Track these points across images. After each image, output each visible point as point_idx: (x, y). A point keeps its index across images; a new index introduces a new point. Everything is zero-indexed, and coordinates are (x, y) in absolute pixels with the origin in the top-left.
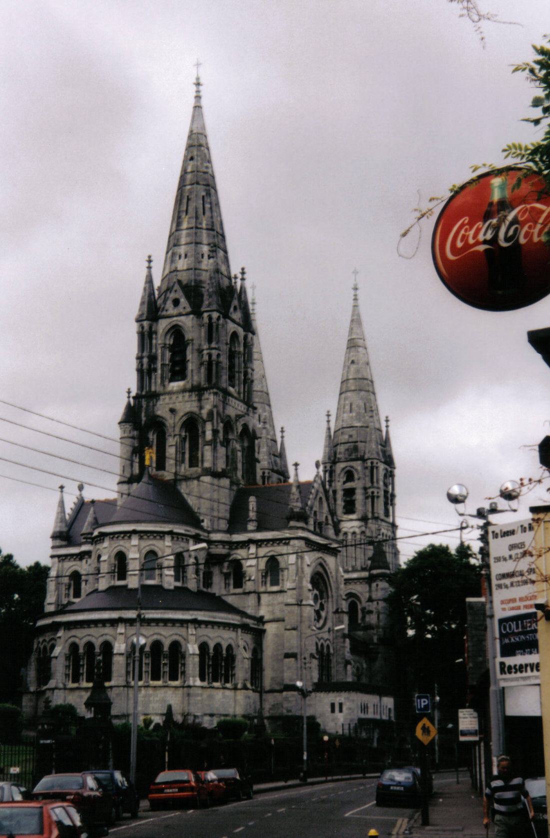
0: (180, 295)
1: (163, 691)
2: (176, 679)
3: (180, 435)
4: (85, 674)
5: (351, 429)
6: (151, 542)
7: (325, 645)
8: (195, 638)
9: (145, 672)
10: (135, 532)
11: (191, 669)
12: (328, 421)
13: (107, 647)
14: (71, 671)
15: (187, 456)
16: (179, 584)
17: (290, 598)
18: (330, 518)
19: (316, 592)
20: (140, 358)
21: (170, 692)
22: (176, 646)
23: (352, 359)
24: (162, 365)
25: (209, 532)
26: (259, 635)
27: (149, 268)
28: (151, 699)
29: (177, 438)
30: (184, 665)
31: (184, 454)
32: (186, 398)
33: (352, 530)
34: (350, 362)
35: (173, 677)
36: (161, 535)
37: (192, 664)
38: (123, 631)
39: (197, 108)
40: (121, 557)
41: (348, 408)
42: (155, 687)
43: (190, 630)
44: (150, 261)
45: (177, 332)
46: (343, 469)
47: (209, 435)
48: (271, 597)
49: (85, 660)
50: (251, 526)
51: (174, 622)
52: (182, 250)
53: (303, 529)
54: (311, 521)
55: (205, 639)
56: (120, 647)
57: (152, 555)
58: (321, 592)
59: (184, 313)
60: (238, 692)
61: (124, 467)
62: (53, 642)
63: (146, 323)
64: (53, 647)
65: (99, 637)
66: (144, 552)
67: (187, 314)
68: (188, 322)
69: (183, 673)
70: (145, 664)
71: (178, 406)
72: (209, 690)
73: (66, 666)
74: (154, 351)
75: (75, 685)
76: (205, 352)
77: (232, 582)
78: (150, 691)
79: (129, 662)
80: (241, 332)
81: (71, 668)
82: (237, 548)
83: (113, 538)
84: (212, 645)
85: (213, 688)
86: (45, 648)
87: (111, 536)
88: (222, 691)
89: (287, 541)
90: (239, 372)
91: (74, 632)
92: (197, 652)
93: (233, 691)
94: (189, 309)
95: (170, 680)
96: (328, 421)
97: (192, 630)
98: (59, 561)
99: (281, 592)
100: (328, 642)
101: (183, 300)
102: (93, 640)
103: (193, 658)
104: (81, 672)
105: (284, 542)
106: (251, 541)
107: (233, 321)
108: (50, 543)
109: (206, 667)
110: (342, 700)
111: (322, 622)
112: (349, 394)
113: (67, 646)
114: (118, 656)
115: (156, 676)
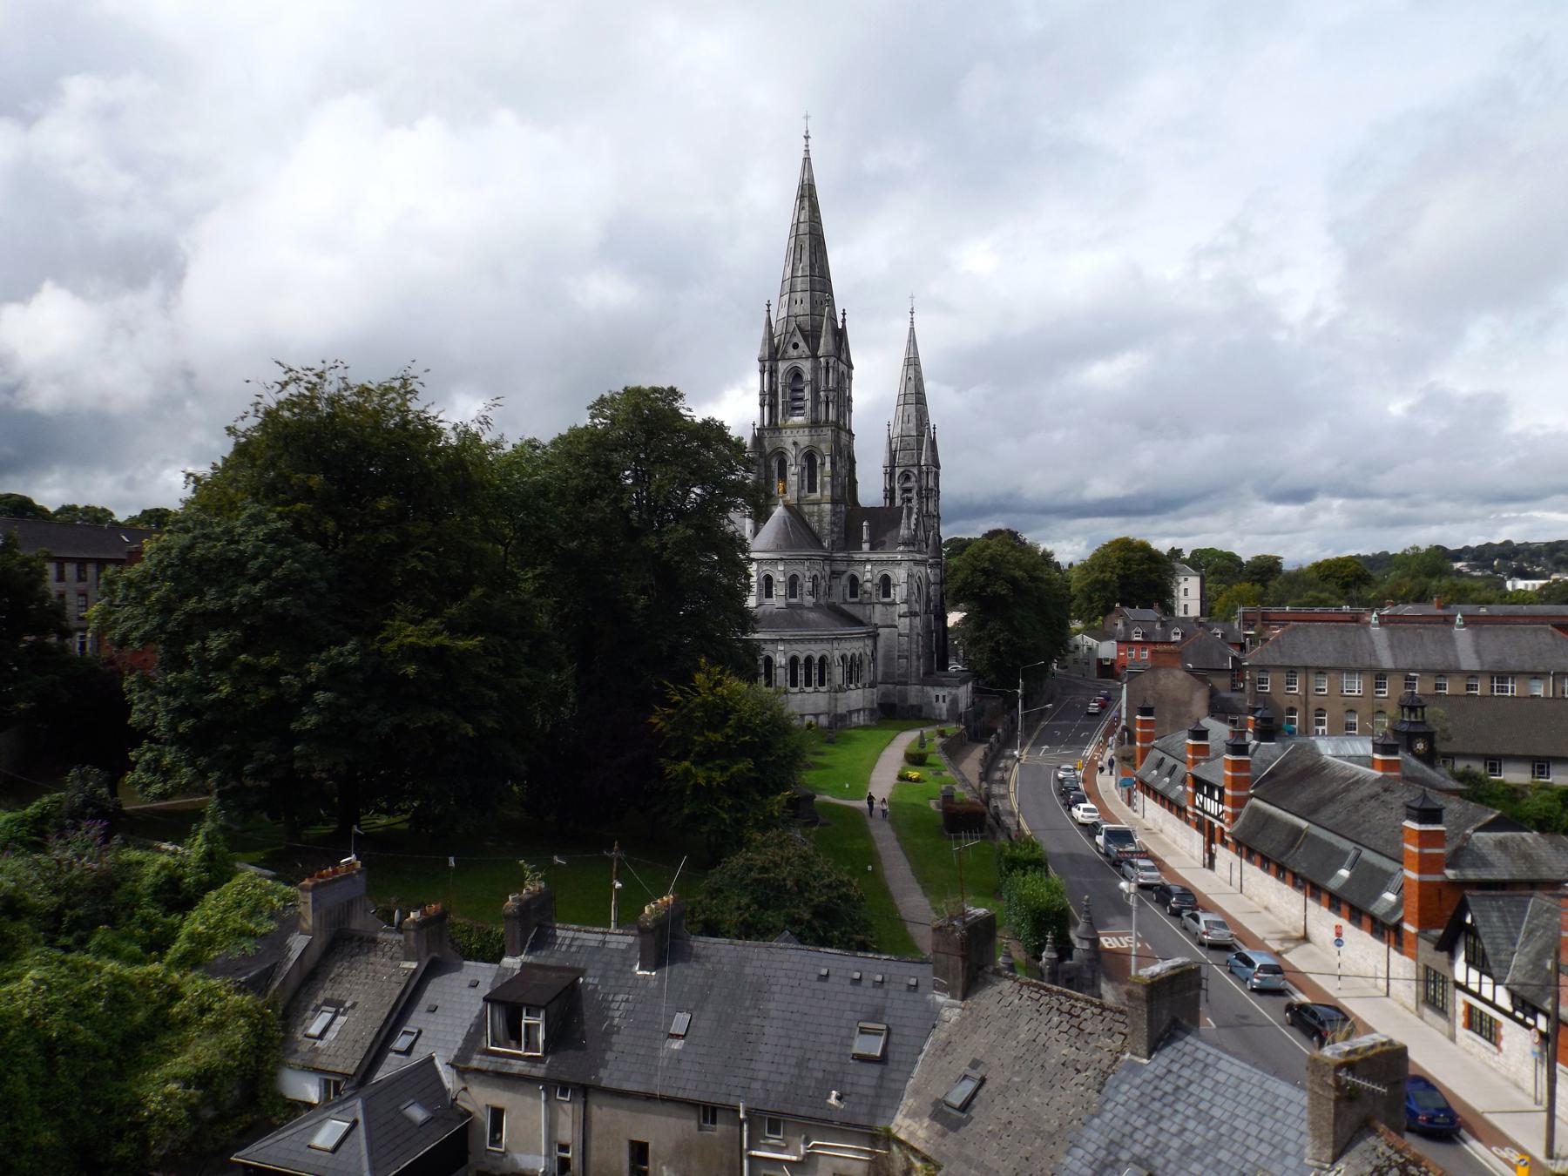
0: (798, 339)
10: (781, 559)
15: (806, 482)
20: (762, 394)
22: (823, 659)
27: (769, 311)
31: (803, 481)
32: (807, 433)
35: (822, 683)
36: (801, 561)
37: (838, 674)
38: (782, 648)
39: (807, 160)
40: (769, 579)
41: (906, 419)
44: (769, 306)
46: (902, 473)
47: (828, 466)
50: (866, 547)
52: (798, 296)
60: (866, 690)
66: (789, 575)
67: (807, 358)
68: (806, 366)
71: (798, 439)
74: (774, 387)
76: (822, 393)
77: (848, 592)
82: (854, 565)
97: (835, 645)
101: (802, 344)
106: (868, 561)
110: (946, 694)
112: (906, 407)
115: (808, 684)
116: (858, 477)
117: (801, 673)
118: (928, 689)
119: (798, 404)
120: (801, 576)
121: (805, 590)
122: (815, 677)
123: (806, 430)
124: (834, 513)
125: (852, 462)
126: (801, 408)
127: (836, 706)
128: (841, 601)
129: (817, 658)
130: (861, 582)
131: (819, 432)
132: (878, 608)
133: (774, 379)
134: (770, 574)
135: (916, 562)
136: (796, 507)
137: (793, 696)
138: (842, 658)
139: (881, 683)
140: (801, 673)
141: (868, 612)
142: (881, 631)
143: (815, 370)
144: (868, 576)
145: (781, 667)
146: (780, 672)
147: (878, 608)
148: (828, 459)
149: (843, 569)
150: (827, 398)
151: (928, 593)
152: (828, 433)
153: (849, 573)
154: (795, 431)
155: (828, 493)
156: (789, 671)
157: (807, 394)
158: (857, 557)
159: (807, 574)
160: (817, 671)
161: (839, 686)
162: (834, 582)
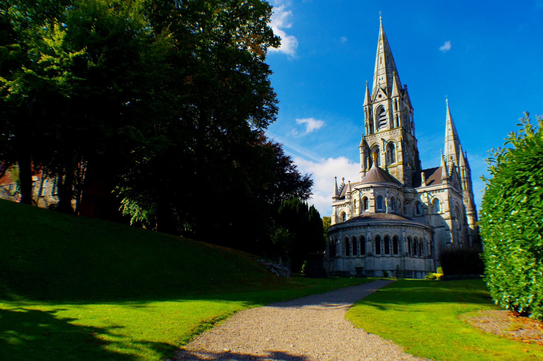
1: (391, 258)
3: (387, 150)
4: (352, 252)
10: (372, 187)
14: (345, 250)
16: (393, 211)
21: (394, 259)
22: (395, 238)
26: (432, 233)
28: (386, 263)
30: (400, 246)
32: (388, 134)
35: (396, 252)
38: (370, 230)
40: (366, 199)
42: (387, 257)
45: (381, 109)
49: (352, 245)
50: (423, 185)
59: (384, 99)
60: (426, 260)
62: (337, 237)
64: (336, 240)
66: (377, 196)
69: (400, 250)
73: (343, 248)
74: (372, 117)
75: (348, 257)
77: (416, 211)
80: (408, 108)
81: (345, 249)
86: (332, 240)
88: (419, 259)
89: (443, 190)
91: (346, 232)
92: (407, 240)
93: (424, 260)
94: (386, 97)
101: (383, 95)
102: (356, 235)
106: (425, 192)
107: (405, 102)
114: (368, 242)
115: (387, 252)
116: (421, 158)
117: (382, 246)
123: (388, 132)
124: (405, 170)
125: (417, 152)
126: (385, 124)
127: (404, 265)
128: (412, 216)
129: (392, 236)
131: (394, 132)
133: (371, 114)
136: (385, 169)
137: (377, 259)
138: (408, 238)
140: (382, 246)
141: (427, 220)
142: (436, 230)
143: (390, 105)
145: (369, 241)
146: (368, 244)
148: (400, 144)
152: (399, 132)
153: (415, 200)
154: (382, 134)
155: (401, 160)
156: (375, 245)
157: (388, 116)
158: (419, 190)
160: (392, 245)
161: (406, 253)
162: (407, 206)
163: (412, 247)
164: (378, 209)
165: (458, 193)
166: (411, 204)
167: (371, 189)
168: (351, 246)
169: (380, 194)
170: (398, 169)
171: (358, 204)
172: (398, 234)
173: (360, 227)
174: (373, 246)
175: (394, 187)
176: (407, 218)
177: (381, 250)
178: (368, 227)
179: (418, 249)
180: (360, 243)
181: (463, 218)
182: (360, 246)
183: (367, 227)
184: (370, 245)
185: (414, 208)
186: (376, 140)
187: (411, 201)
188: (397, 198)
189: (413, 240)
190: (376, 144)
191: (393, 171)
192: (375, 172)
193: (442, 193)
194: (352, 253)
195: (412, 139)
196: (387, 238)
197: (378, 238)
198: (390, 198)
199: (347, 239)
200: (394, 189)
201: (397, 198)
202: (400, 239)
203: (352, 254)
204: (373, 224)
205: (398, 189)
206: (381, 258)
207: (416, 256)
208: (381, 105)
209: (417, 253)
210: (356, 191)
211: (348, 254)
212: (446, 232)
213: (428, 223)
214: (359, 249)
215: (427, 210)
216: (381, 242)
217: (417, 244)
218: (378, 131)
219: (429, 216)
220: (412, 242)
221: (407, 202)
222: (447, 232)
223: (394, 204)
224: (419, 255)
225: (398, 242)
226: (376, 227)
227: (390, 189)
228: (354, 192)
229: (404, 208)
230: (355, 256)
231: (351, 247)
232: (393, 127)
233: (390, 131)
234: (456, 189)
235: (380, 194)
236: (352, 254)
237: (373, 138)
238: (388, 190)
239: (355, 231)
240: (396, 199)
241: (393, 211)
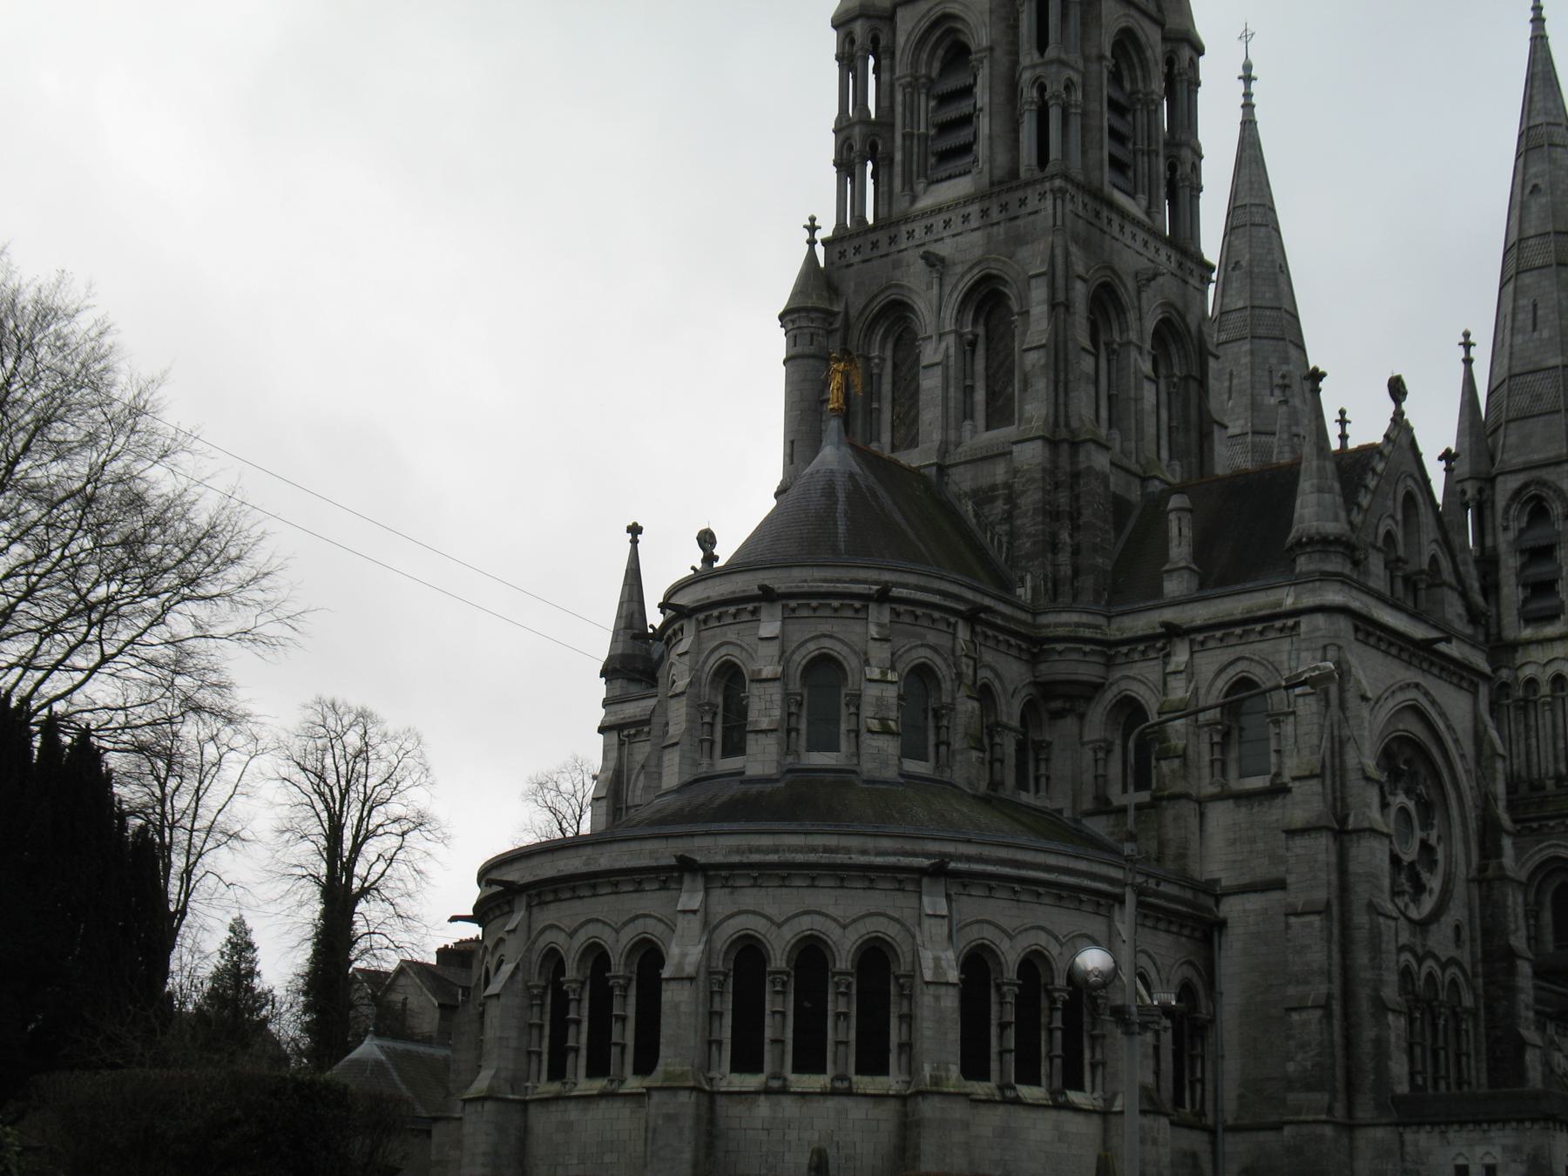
1: (832, 1103)
2: (883, 1070)
3: (960, 336)
4: (583, 1052)
5: (1540, 375)
6: (825, 627)
7: (1444, 978)
8: (946, 930)
9: (774, 1041)
10: (768, 595)
11: (928, 1033)
12: (1468, 361)
13: (649, 956)
15: (980, 396)
17: (1305, 804)
18: (1445, 564)
19: (1400, 799)
21: (857, 1111)
23: (1534, 182)
24: (904, 136)
25: (1035, 614)
29: (951, 340)
30: (908, 1019)
31: (969, 390)
32: (974, 223)
33: (1550, 671)
34: (1527, 191)
35: (872, 1059)
40: (730, 676)
41: (1525, 318)
42: (803, 1095)
43: (925, 900)
46: (1518, 493)
48: (1242, 814)
49: (586, 1004)
51: (869, 875)
53: (1343, 580)
54: (1376, 563)
55: (989, 934)
56: (684, 955)
57: (825, 669)
58: (1425, 807)
61: (792, 442)
63: (859, 28)
65: (625, 924)
66: (800, 659)
69: (907, 1047)
70: (774, 1013)
72: (1001, 1110)
76: (1027, 76)
77: (1115, 769)
78: (789, 1106)
79: (717, 1007)
83: (705, 621)
84: (1011, 955)
85: (1018, 1102)
87: (701, 616)
89: (1290, 622)
90: (1150, 153)
92: (953, 976)
95: (860, 1070)
96: (1468, 361)
97: (934, 903)
98: (621, 744)
99: (1277, 791)
100: (1453, 970)
102: (607, 937)
103: (937, 998)
104: (571, 1043)
105: (1278, 624)
106: (1172, 632)
108: (600, 688)
109: (994, 1031)
110: (1496, 1156)
111: (1428, 903)
112: (1527, 279)
113: (536, 958)
114: (673, 985)
115: (809, 1057)
118: (1421, 1139)
119: (961, 137)
120: (851, 663)
121: (867, 711)
122: (841, 1032)
123: (974, 209)
128: (1087, 804)
130: (1154, 718)
132: (1220, 816)
134: (737, 657)
135: (1366, 628)
139: (1235, 1129)
144: (1179, 690)
146: (674, 998)
147: (1220, 816)
149: (1088, 671)
150: (1042, 89)
151: (1486, 802)
153: (1110, 696)
154: (938, 221)
156: (727, 1005)
159: (879, 653)
163: (1003, 1026)
164: (811, 748)
165: (1427, 645)
166: (1082, 717)
167: (763, 615)
168: (581, 1011)
169: (827, 643)
170: (1015, 472)
171: (678, 716)
172: (892, 931)
173: (637, 877)
174: (713, 1015)
175: (936, 599)
176: (1050, 826)
177: (767, 1047)
178: (687, 878)
179: (1051, 1045)
180: (633, 992)
181: (1473, 825)
182: (631, 1012)
183: (680, 881)
184: (683, 1008)
185: (1109, 751)
186: (897, 265)
187: (1089, 699)
188: (959, 675)
189: (1011, 973)
190: (893, 295)
191: (985, 482)
192: (830, 492)
193: (1285, 645)
194: (583, 1061)
195: (1165, 258)
196: (811, 953)
197: (748, 953)
198: (891, 676)
199: (553, 960)
200: (937, 615)
201: (959, 675)
202: (904, 967)
203: (579, 1064)
204: (719, 859)
205: (973, 616)
206: (762, 1098)
207: (1027, 1092)
208: (947, 17)
209: (1044, 1070)
210: (676, 626)
211: (557, 1072)
212: (1288, 926)
213: (1182, 856)
214: (625, 1034)
215: (1176, 763)
216: (831, 990)
217: (1044, 1003)
218: (914, 199)
219: (1189, 808)
220: (1002, 996)
221: (1057, 705)
222: (1293, 920)
223: (937, 716)
224: (1058, 1082)
225: (893, 989)
226: (738, 884)
227: (901, 608)
228: (670, 632)
229: (1031, 751)
230: (598, 1085)
231: (578, 1022)
232: (1014, 173)
233: (986, 204)
234: (1416, 616)
235: (827, 643)
236: (579, 1064)
237: (883, 250)
238: (885, 615)
239: (605, 906)
240: (947, 686)
241: (913, 766)
